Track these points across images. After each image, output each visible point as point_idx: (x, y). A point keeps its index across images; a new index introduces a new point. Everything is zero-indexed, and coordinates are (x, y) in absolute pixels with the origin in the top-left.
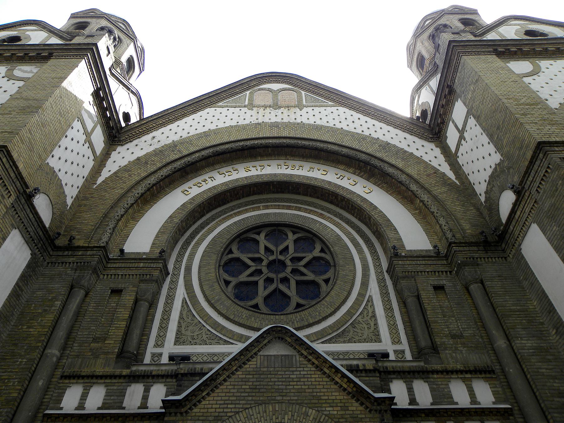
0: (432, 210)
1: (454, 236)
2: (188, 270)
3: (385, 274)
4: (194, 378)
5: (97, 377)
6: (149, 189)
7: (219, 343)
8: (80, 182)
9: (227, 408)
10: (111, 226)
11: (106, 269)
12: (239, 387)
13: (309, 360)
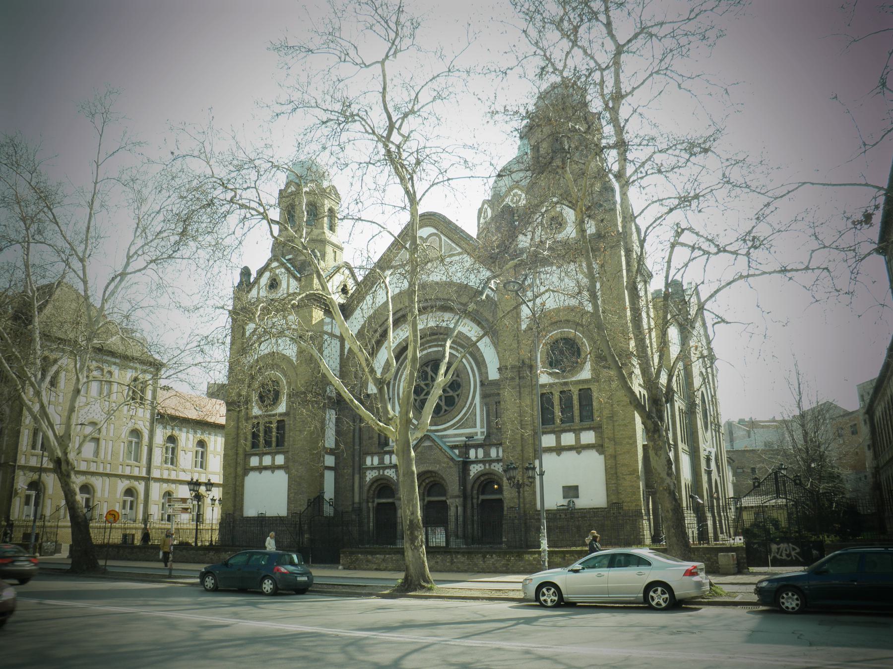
8: (338, 361)
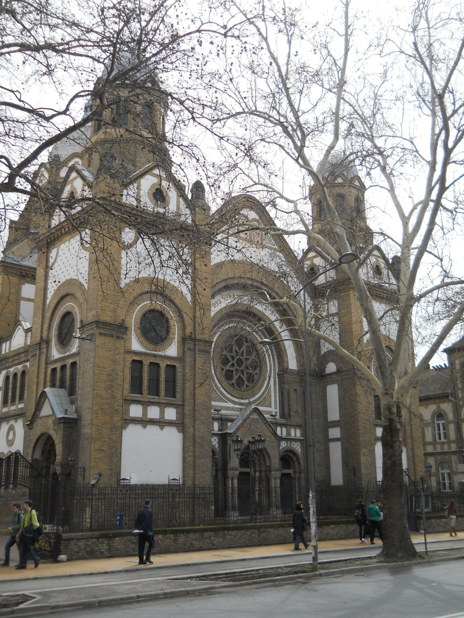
7: (223, 402)
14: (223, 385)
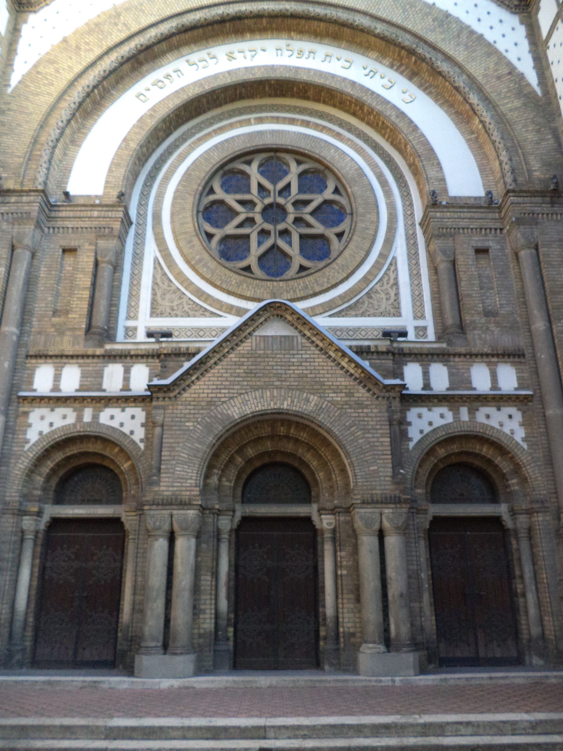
0: (494, 138)
1: (515, 180)
2: (157, 217)
3: (418, 227)
4: (179, 359)
5: (67, 356)
6: (88, 95)
7: (204, 315)
9: (220, 393)
10: (46, 158)
11: (50, 219)
12: (233, 371)
13: (313, 342)
14: (204, 271)
